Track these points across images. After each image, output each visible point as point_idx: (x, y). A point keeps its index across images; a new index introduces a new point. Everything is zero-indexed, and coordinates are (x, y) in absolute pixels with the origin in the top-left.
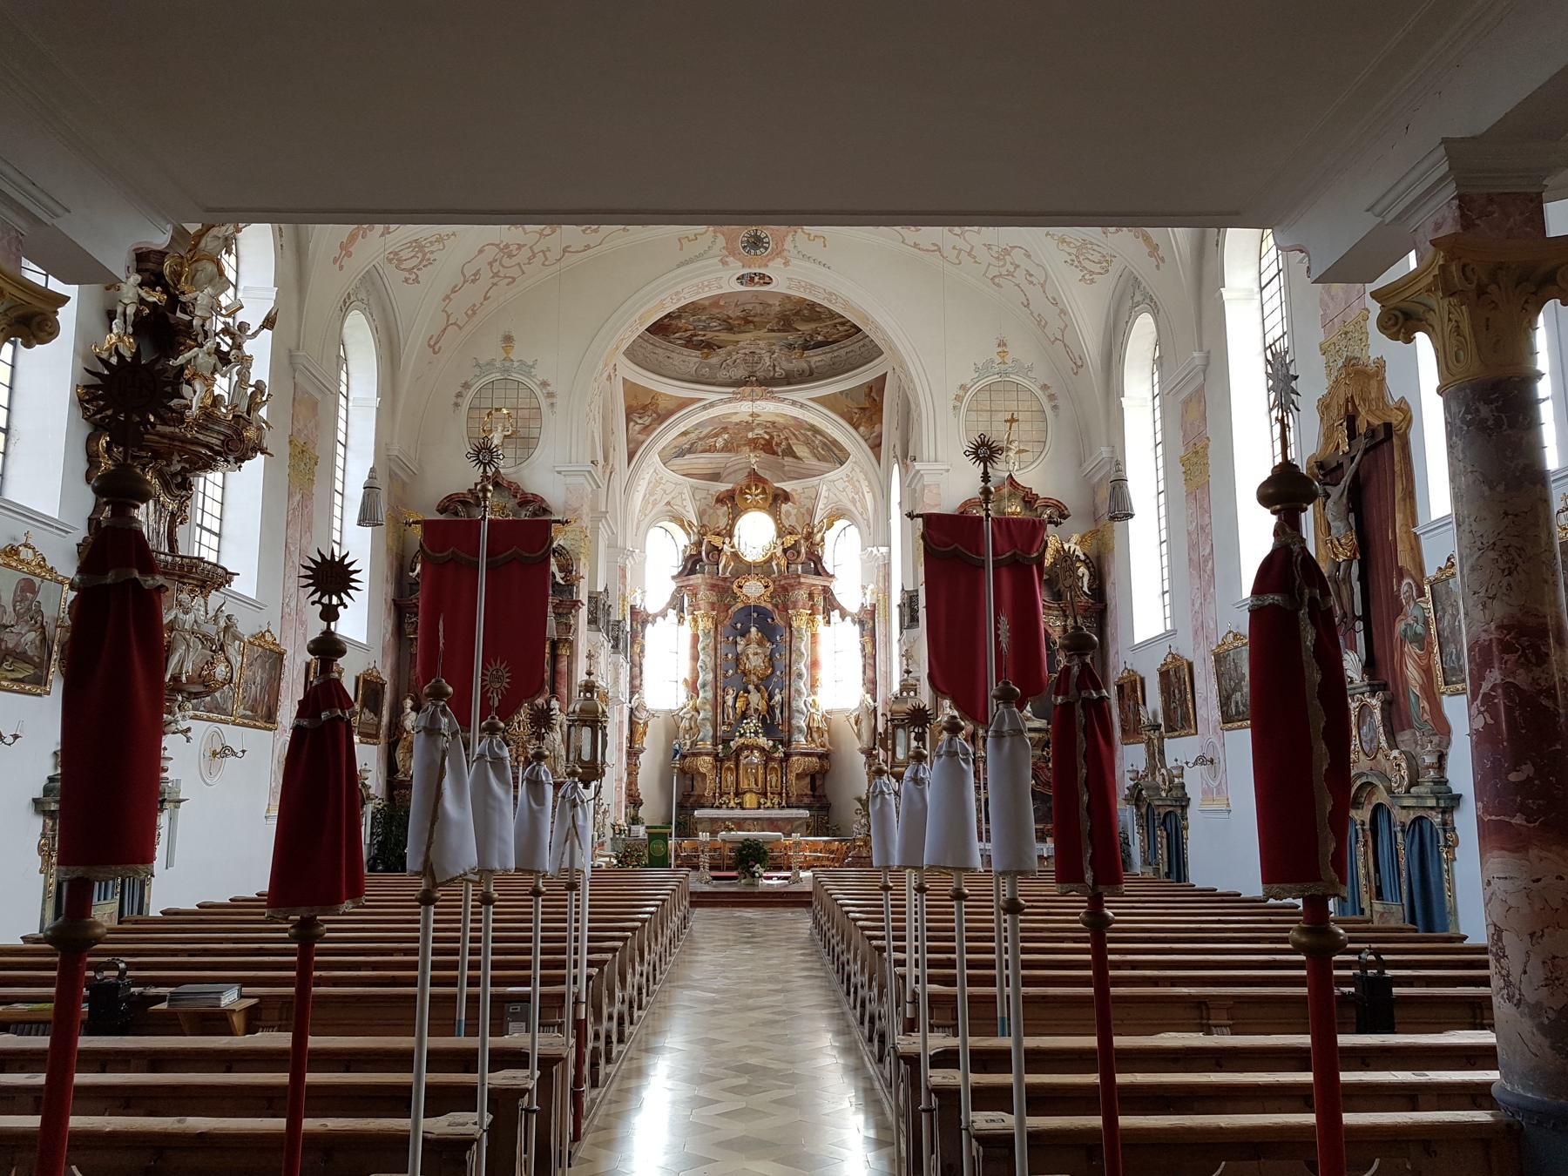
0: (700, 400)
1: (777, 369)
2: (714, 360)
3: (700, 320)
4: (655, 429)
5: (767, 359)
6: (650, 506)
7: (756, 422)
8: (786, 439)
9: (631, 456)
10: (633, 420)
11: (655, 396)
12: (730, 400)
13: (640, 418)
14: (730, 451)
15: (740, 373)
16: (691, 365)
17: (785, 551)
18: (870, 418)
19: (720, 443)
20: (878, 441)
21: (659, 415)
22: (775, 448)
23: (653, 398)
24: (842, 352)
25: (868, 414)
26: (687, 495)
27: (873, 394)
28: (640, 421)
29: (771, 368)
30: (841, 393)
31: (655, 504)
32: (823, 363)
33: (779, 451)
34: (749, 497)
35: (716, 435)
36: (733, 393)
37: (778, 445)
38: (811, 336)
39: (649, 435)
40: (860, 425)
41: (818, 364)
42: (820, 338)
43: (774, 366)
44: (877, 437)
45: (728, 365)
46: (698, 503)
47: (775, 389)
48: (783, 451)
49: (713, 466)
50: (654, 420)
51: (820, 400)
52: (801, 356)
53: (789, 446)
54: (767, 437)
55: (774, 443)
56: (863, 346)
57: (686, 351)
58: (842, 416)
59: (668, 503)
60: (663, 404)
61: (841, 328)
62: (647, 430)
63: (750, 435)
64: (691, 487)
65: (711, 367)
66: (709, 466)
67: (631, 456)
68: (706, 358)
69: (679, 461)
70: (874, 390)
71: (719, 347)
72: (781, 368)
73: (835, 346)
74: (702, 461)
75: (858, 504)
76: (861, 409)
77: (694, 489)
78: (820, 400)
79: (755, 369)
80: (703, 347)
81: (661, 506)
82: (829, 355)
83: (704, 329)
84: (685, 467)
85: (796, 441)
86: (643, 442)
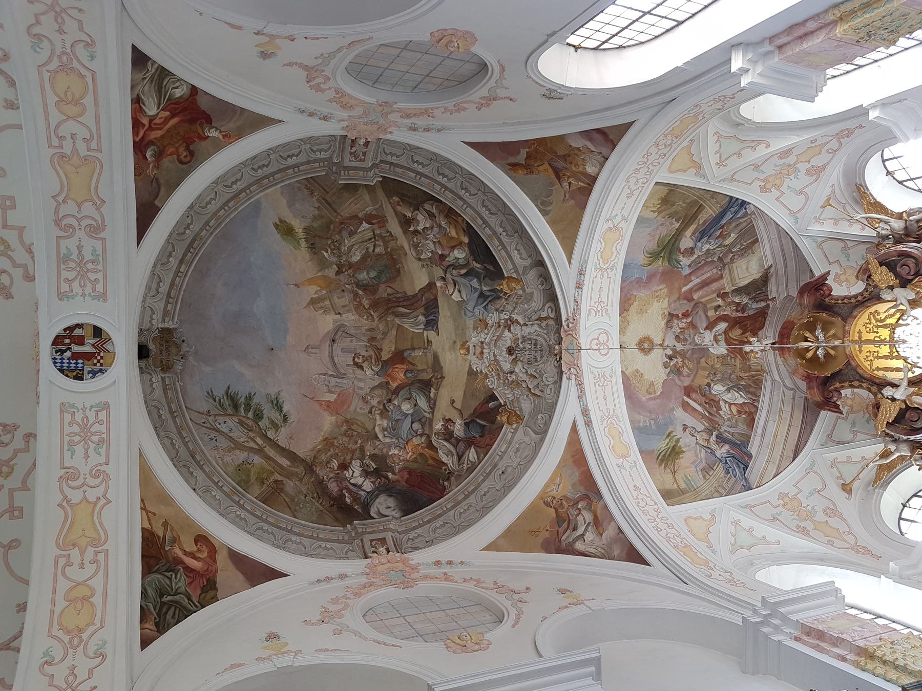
0: (574, 429)
1: (544, 315)
2: (526, 406)
3: (393, 431)
4: (606, 507)
5: (527, 330)
6: (834, 522)
7: (670, 341)
8: (723, 296)
9: (635, 556)
10: (571, 544)
11: (544, 500)
12: (580, 384)
13: (574, 530)
14: (758, 384)
15: (549, 368)
16: (527, 440)
17: (904, 283)
18: (565, 158)
19: (739, 398)
20: (597, 136)
21: (585, 497)
22: (751, 312)
23: (547, 504)
24: (492, 220)
25: (560, 164)
26: (841, 454)
27: (521, 158)
28: (580, 531)
29: (544, 324)
30: (544, 213)
31: (833, 512)
32: (520, 247)
33: (756, 306)
34: (820, 353)
35: (713, 403)
36: (569, 379)
37: (740, 307)
38: (454, 266)
39: (612, 518)
40: (586, 175)
41: (524, 255)
42: (459, 254)
43: (540, 319)
44: (591, 140)
45: (537, 386)
46: (860, 436)
47: (564, 318)
48: (755, 299)
49: (788, 408)
50: (589, 507)
51: (569, 245)
52: (517, 281)
53: (739, 291)
54: (723, 326)
55: (739, 314)
56: (466, 189)
57: (499, 446)
58: (583, 207)
59: (846, 488)
60: (566, 488)
61: (423, 222)
62: (601, 520)
63: (721, 349)
64: (824, 445)
65: (535, 412)
66: (786, 415)
67: (635, 556)
68: (520, 418)
69: (756, 468)
70: (512, 160)
71: (493, 397)
72: (542, 309)
73: (485, 234)
74: (771, 428)
75: (817, 162)
76: (558, 178)
77: (831, 440)
78: (569, 245)
79: (545, 347)
80: (493, 421)
81: (848, 506)
82: (505, 240)
83: (426, 422)
84: (777, 454)
85: (724, 281)
86: (620, 530)
